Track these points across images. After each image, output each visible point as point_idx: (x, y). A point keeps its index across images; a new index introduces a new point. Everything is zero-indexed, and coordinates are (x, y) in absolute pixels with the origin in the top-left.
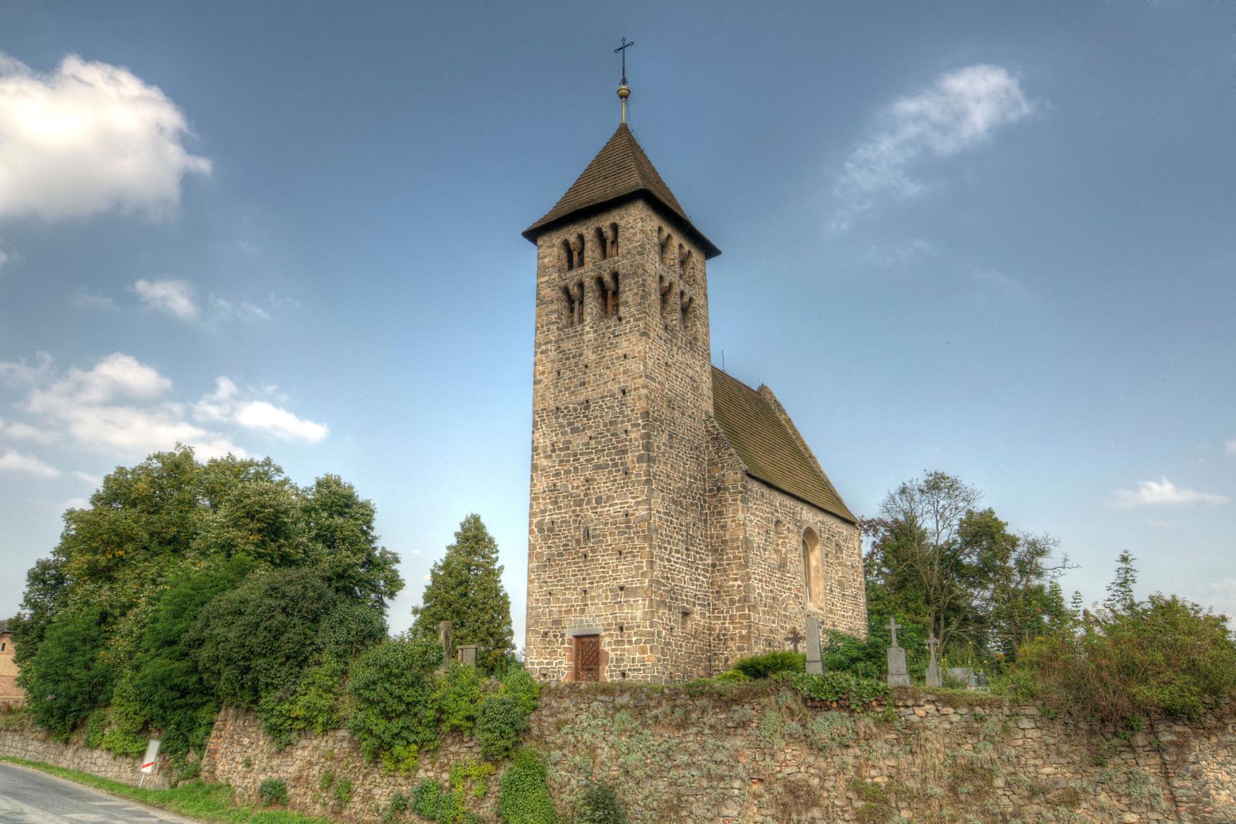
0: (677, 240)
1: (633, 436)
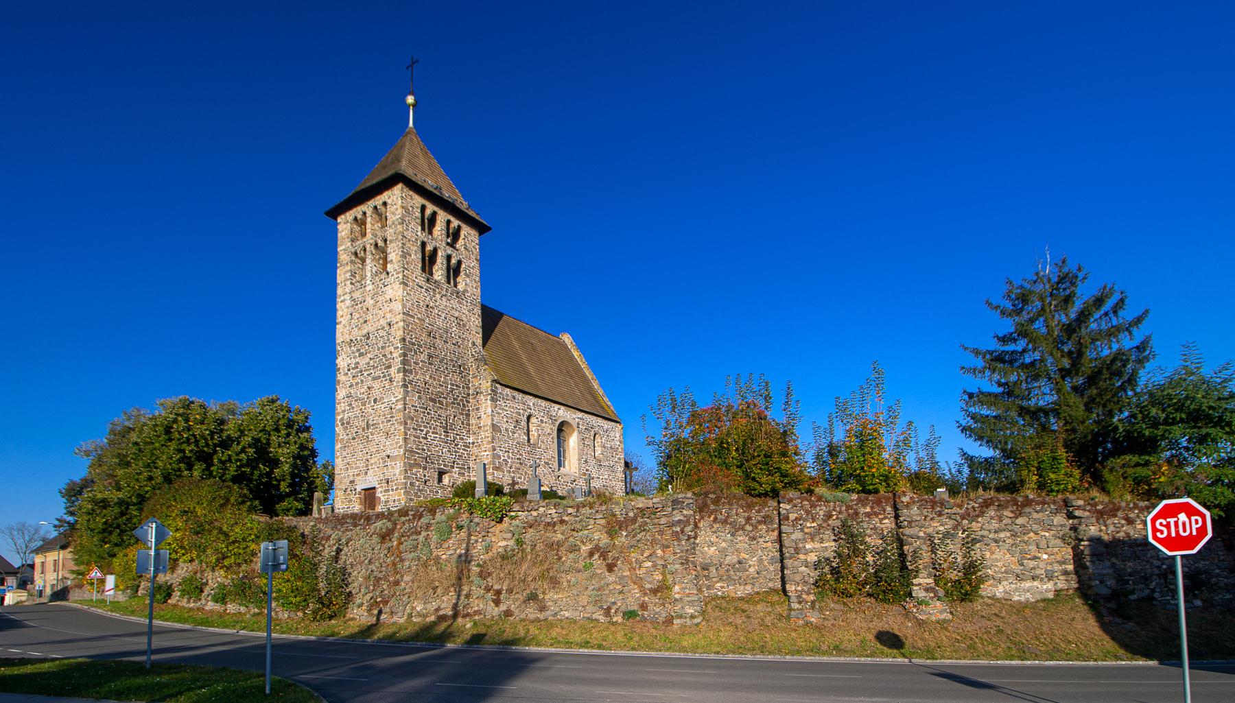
0: (442, 216)
1: (395, 355)
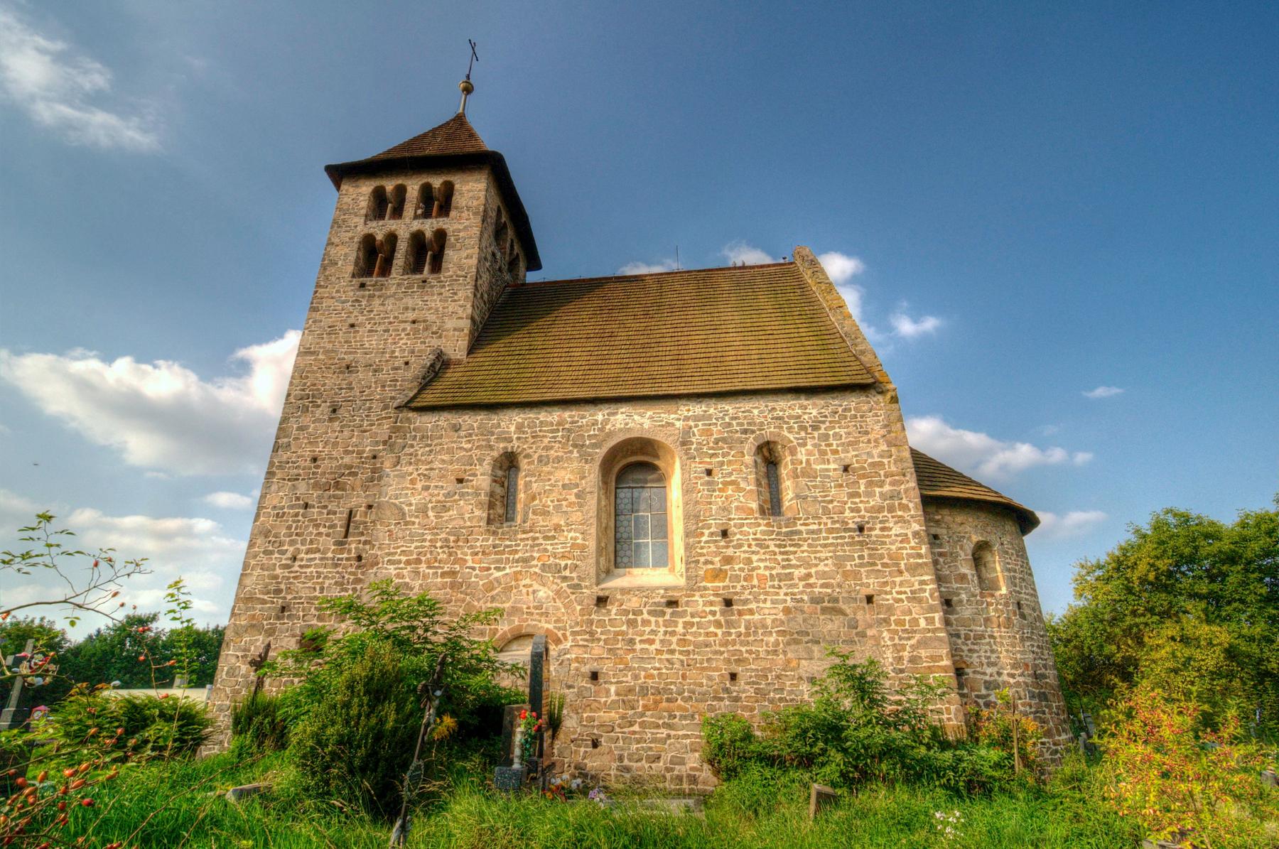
0: (413, 187)
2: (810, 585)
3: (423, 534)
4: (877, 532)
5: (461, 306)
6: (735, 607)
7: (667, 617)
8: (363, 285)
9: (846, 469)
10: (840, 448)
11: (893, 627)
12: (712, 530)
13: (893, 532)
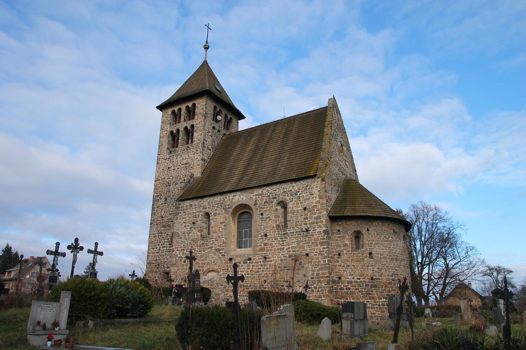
2: (289, 251)
3: (185, 241)
4: (312, 231)
5: (199, 156)
6: (267, 260)
7: (248, 264)
8: (171, 152)
9: (305, 209)
10: (303, 202)
11: (313, 264)
12: (262, 235)
13: (317, 231)
